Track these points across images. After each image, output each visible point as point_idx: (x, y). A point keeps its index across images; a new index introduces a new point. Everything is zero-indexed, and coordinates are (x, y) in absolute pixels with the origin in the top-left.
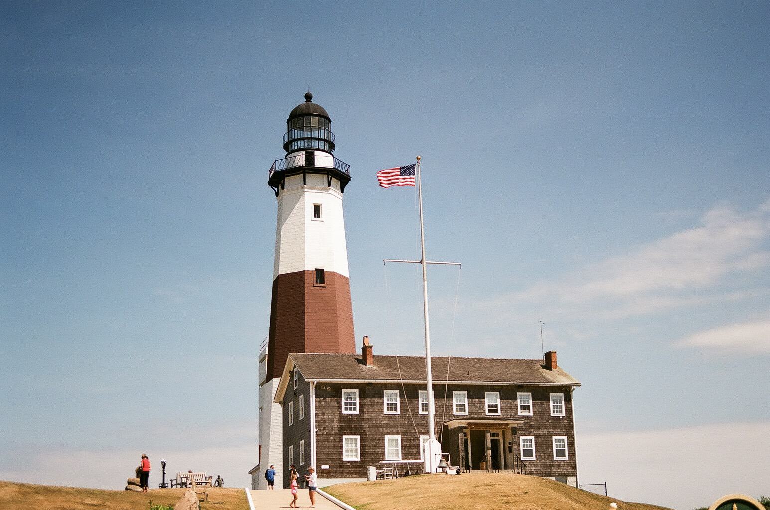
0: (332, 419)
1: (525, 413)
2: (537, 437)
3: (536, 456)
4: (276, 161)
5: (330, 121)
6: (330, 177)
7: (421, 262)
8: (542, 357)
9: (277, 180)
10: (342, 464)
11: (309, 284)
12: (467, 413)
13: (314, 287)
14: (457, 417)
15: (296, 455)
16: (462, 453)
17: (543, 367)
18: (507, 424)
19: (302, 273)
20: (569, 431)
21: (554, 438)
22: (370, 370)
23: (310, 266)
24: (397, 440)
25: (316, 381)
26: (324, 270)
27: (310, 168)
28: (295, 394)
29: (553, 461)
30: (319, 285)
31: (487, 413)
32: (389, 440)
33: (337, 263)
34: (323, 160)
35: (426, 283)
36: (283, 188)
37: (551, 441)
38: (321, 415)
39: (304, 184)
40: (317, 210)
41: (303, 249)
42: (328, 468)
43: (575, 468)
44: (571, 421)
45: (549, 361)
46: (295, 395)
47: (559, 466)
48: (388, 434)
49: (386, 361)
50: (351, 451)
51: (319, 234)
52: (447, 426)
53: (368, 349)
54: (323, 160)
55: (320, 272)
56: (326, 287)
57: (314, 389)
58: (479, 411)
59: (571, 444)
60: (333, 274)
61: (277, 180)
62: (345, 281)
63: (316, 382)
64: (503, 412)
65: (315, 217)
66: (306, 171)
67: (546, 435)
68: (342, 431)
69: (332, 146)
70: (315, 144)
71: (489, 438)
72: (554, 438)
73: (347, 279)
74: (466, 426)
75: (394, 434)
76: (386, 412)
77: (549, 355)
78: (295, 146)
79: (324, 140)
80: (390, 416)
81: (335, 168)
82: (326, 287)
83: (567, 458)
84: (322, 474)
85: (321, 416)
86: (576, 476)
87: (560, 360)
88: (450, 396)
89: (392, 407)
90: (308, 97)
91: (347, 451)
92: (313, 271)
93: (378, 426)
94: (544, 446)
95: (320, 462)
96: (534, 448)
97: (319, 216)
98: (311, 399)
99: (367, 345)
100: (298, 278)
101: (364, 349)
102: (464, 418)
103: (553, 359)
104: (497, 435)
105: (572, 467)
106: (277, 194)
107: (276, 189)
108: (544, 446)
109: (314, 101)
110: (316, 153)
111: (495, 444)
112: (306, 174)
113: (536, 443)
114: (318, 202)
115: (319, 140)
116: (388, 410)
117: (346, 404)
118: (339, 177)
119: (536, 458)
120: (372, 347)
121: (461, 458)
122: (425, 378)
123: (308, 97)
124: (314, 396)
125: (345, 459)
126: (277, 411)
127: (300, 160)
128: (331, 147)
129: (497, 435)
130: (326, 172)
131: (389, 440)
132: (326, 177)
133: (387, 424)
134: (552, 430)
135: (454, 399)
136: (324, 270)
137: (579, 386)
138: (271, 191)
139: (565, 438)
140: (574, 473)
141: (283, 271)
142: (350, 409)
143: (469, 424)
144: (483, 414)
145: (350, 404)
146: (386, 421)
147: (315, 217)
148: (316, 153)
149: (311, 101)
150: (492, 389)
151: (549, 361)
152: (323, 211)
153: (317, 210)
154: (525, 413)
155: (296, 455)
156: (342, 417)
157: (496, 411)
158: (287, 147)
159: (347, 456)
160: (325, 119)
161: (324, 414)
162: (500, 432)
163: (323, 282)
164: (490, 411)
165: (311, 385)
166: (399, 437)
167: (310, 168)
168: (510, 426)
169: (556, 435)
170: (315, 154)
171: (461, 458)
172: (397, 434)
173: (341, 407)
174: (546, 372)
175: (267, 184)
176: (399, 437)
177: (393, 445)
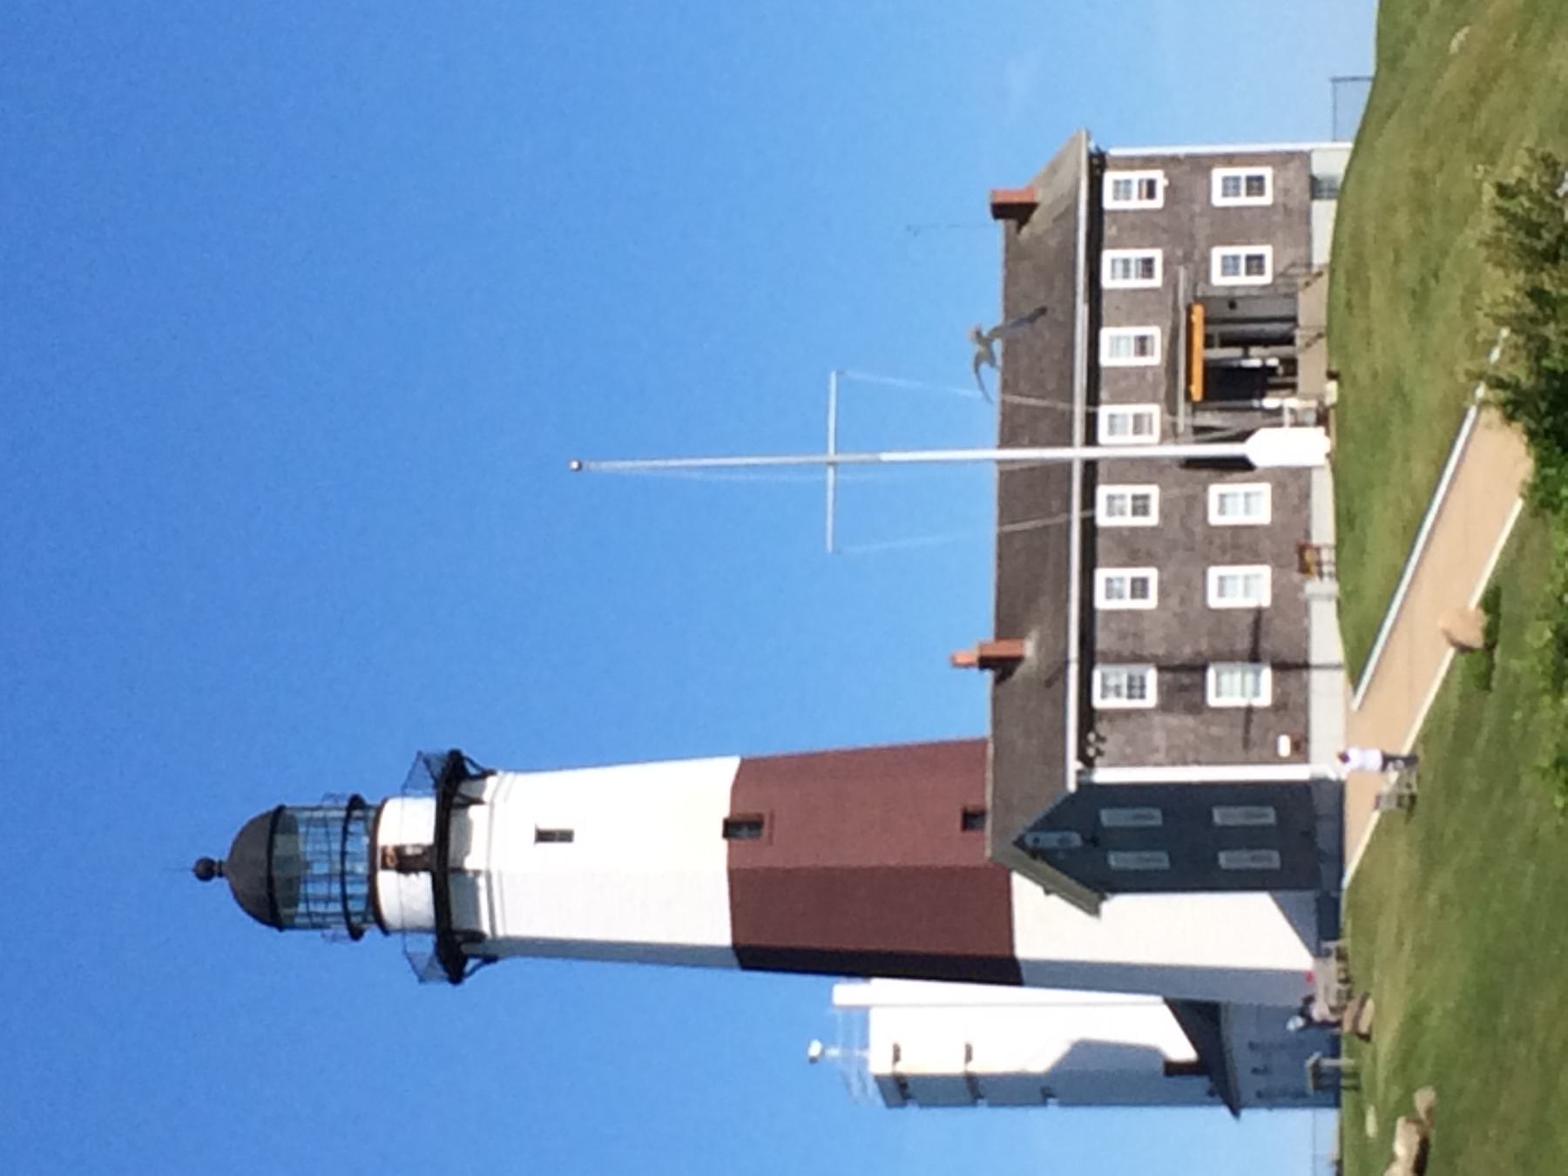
0: (1169, 731)
1: (1158, 267)
5: (280, 809)
7: (833, 464)
8: (998, 230)
10: (1280, 705)
20: (1201, 165)
22: (1039, 647)
25: (1074, 765)
29: (1274, 206)
30: (765, 831)
33: (705, 787)
37: (1226, 209)
43: (1291, 155)
44: (1174, 159)
46: (1097, 840)
59: (1229, 160)
68: (1197, 706)
72: (1218, 200)
73: (745, 766)
77: (1001, 211)
80: (1163, 593)
85: (1160, 756)
89: (1139, 588)
90: (207, 870)
92: (730, 846)
93: (1183, 618)
94: (1232, 226)
100: (746, 888)
106: (489, 959)
108: (1232, 226)
109: (219, 851)
114: (533, 836)
118: (454, 784)
123: (207, 870)
133: (1183, 601)
138: (480, 978)
140: (1305, 157)
145: (1130, 687)
146: (1173, 602)
149: (221, 863)
154: (1158, 267)
156: (1165, 706)
160: (278, 822)
161: (1156, 750)
166: (1214, 573)
173: (1141, 712)
176: (1214, 573)
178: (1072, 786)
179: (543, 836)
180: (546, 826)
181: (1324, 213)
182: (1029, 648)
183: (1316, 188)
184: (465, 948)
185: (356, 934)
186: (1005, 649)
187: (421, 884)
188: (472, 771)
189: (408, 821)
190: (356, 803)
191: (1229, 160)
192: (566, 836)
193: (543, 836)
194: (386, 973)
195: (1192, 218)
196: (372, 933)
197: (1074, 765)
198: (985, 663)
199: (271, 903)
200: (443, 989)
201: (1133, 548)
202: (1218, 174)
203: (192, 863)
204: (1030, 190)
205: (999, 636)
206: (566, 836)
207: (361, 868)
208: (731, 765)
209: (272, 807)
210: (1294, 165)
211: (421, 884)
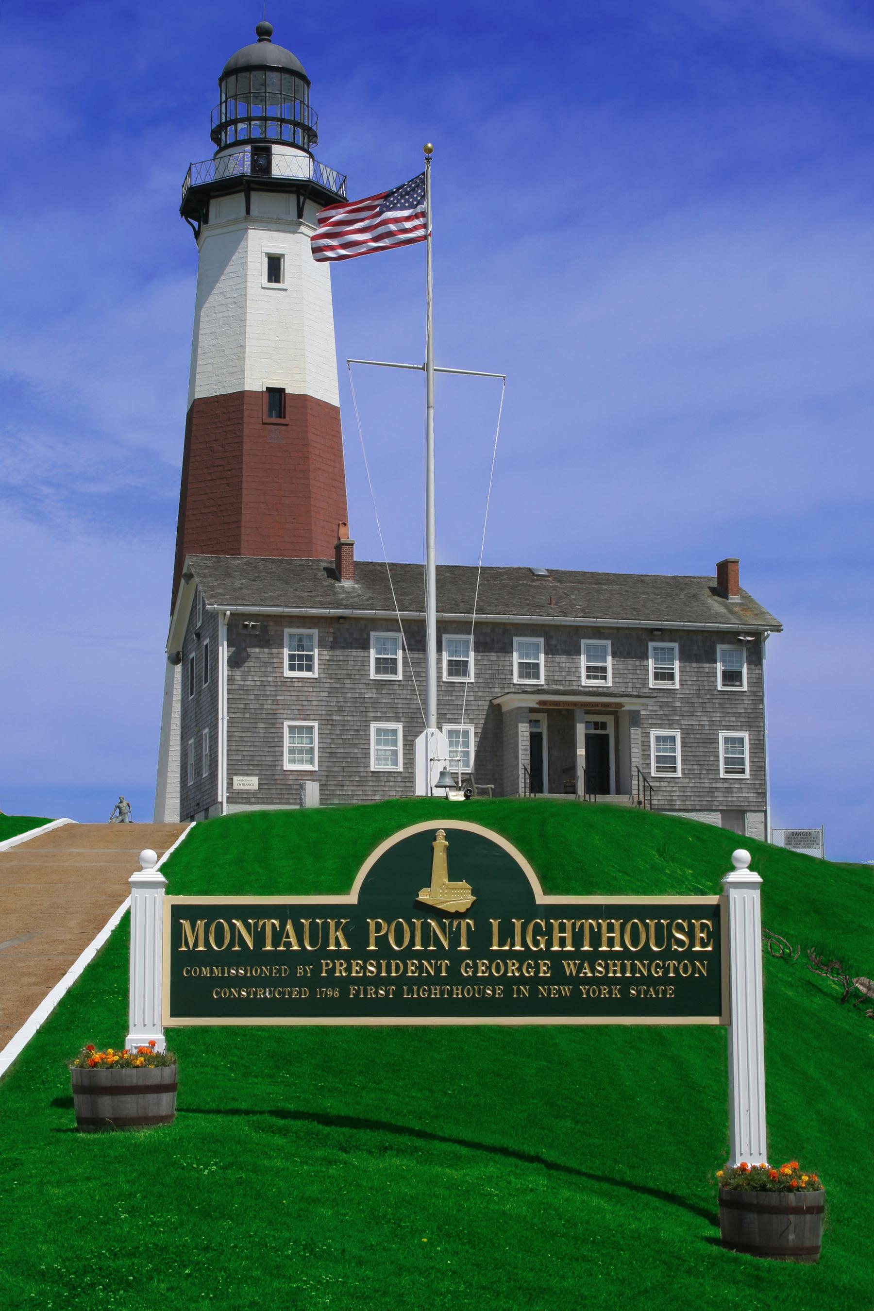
1: (665, 685)
2: (686, 735)
3: (683, 769)
4: (191, 164)
5: (308, 83)
6: (302, 199)
7: (425, 368)
9: (197, 204)
11: (253, 418)
12: (542, 681)
13: (264, 424)
14: (523, 690)
15: (199, 758)
16: (524, 758)
17: (714, 591)
18: (620, 705)
19: (240, 396)
21: (722, 735)
23: (256, 381)
24: (394, 732)
25: (229, 610)
26: (284, 389)
27: (261, 181)
28: (198, 635)
30: (274, 420)
31: (584, 682)
32: (378, 731)
33: (317, 378)
35: (432, 411)
36: (206, 222)
37: (716, 741)
38: (238, 678)
39: (248, 212)
40: (275, 267)
41: (243, 347)
42: (316, 785)
45: (724, 581)
47: (729, 790)
48: (377, 719)
49: (371, 573)
50: (301, 751)
51: (285, 321)
52: (499, 705)
53: (345, 549)
54: (289, 163)
55: (277, 395)
56: (287, 425)
57: (226, 627)
58: (569, 678)
59: (758, 747)
60: (304, 399)
62: (330, 413)
63: (228, 613)
64: (617, 680)
65: (270, 280)
66: (253, 186)
67: (707, 727)
69: (311, 134)
70: (273, 130)
71: (581, 731)
72: (722, 735)
73: (336, 409)
74: (534, 705)
75: (388, 719)
76: (373, 676)
77: (724, 568)
78: (229, 135)
81: (309, 181)
82: (287, 425)
83: (747, 775)
86: (765, 812)
87: (746, 581)
88: (507, 649)
91: (292, 751)
92: (262, 392)
95: (234, 770)
96: (678, 754)
97: (278, 281)
98: (220, 648)
99: (343, 540)
101: (339, 548)
102: (539, 691)
103: (731, 575)
104: (604, 726)
105: (758, 793)
106: (197, 234)
107: (196, 224)
110: (276, 149)
111: (598, 746)
113: (684, 744)
114: (275, 250)
115: (282, 121)
116: (378, 671)
117: (292, 657)
119: (683, 773)
120: (352, 544)
121: (521, 771)
122: (422, 606)
124: (225, 643)
125: (288, 766)
126: (178, 668)
127: (240, 162)
128: (306, 138)
129: (604, 726)
130: (294, 189)
131: (378, 731)
132: (293, 198)
134: (718, 719)
135: (515, 654)
136: (284, 389)
137: (778, 631)
138: (184, 228)
141: (201, 393)
142: (300, 668)
143: (541, 703)
144: (575, 683)
145: (300, 657)
146: (371, 695)
147: (270, 280)
148: (276, 149)
150: (598, 632)
151: (724, 581)
152: (288, 268)
153: (275, 267)
155: (199, 758)
158: (216, 135)
159: (292, 761)
162: (610, 720)
163: (281, 414)
165: (220, 619)
166: (399, 727)
168: (626, 708)
169: (728, 728)
170: (273, 152)
171: (521, 771)
172: (397, 719)
174: (715, 604)
175: (179, 213)
177: (386, 743)
191: (758, 747)
195: (705, 712)
200: (177, 200)
202: (745, 735)
204: (739, 591)
207: (256, 134)
210: (752, 796)
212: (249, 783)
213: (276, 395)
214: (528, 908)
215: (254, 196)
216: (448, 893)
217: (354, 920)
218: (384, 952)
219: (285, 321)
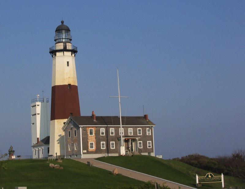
8: (142, 115)
34: (69, 46)
36: (56, 56)
61: (53, 52)
72: (148, 142)
76: (101, 135)
79: (69, 39)
80: (102, 136)
83: (151, 147)
84: (84, 153)
89: (103, 133)
90: (62, 22)
107: (52, 54)
109: (65, 24)
112: (65, 52)
114: (68, 61)
115: (68, 39)
118: (74, 51)
123: (62, 22)
127: (60, 46)
132: (70, 53)
138: (50, 55)
139: (151, 142)
140: (153, 152)
157: (131, 134)
160: (68, 30)
164: (130, 134)
167: (65, 50)
178: (80, 126)
179: (68, 62)
180: (69, 63)
181: (146, 154)
182: (95, 120)
183: (149, 153)
184: (54, 54)
185: (55, 40)
186: (95, 118)
187: (62, 48)
188: (75, 54)
189: (69, 46)
190: (71, 40)
192: (68, 65)
193: (68, 62)
194: (51, 44)
196: (55, 42)
197: (82, 126)
198: (93, 115)
199: (59, 30)
201: (107, 132)
202: (151, 142)
203: (63, 20)
205: (96, 117)
206: (68, 65)
208: (77, 85)
209: (70, 30)
211: (62, 48)
212: (85, 151)
213: (70, 85)
214: (213, 177)
215: (65, 52)
216: (210, 176)
217: (206, 178)
218: (207, 179)
219: (65, 70)
